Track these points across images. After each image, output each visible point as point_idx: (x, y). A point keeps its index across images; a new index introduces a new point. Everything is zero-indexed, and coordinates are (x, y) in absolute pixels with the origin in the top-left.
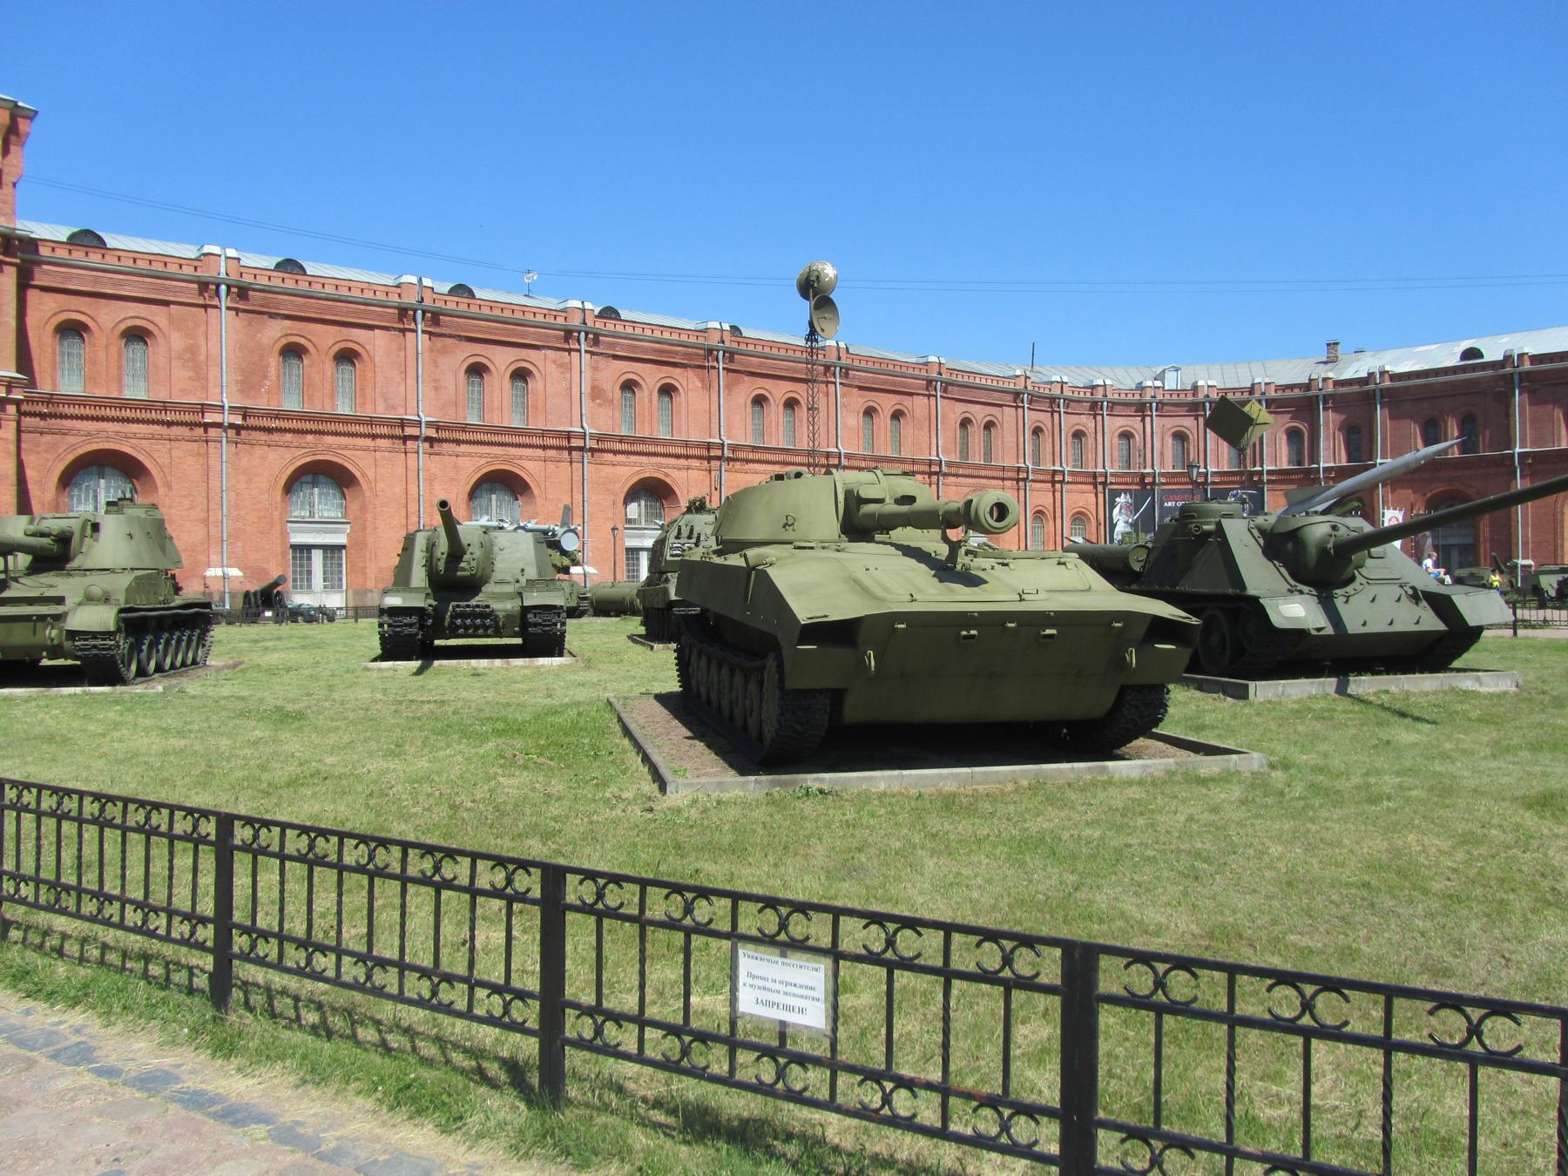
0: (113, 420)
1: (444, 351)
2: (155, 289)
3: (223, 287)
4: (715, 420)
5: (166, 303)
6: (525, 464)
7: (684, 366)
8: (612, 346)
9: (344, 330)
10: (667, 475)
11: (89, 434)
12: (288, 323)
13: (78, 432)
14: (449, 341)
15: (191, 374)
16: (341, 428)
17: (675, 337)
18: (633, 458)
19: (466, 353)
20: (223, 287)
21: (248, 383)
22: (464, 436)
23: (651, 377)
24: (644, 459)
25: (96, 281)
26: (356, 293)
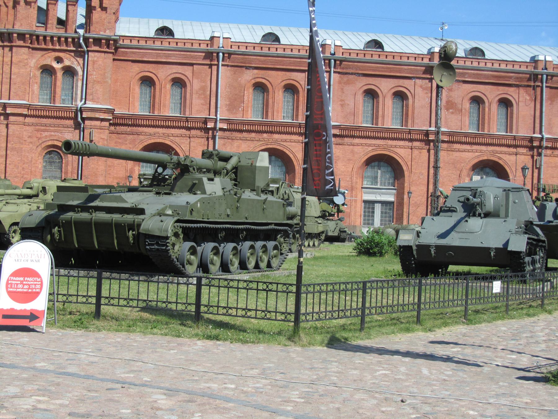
0: (162, 127)
1: (348, 83)
2: (186, 57)
3: (221, 54)
4: (537, 121)
5: (192, 65)
6: (398, 150)
8: (463, 75)
9: (288, 74)
10: (500, 158)
11: (150, 135)
12: (256, 71)
13: (146, 134)
14: (351, 76)
15: (202, 101)
16: (282, 129)
17: (510, 67)
18: (475, 147)
19: (362, 83)
20: (221, 54)
21: (232, 106)
22: (357, 133)
23: (491, 95)
24: (483, 148)
25: (158, 55)
26: (295, 52)
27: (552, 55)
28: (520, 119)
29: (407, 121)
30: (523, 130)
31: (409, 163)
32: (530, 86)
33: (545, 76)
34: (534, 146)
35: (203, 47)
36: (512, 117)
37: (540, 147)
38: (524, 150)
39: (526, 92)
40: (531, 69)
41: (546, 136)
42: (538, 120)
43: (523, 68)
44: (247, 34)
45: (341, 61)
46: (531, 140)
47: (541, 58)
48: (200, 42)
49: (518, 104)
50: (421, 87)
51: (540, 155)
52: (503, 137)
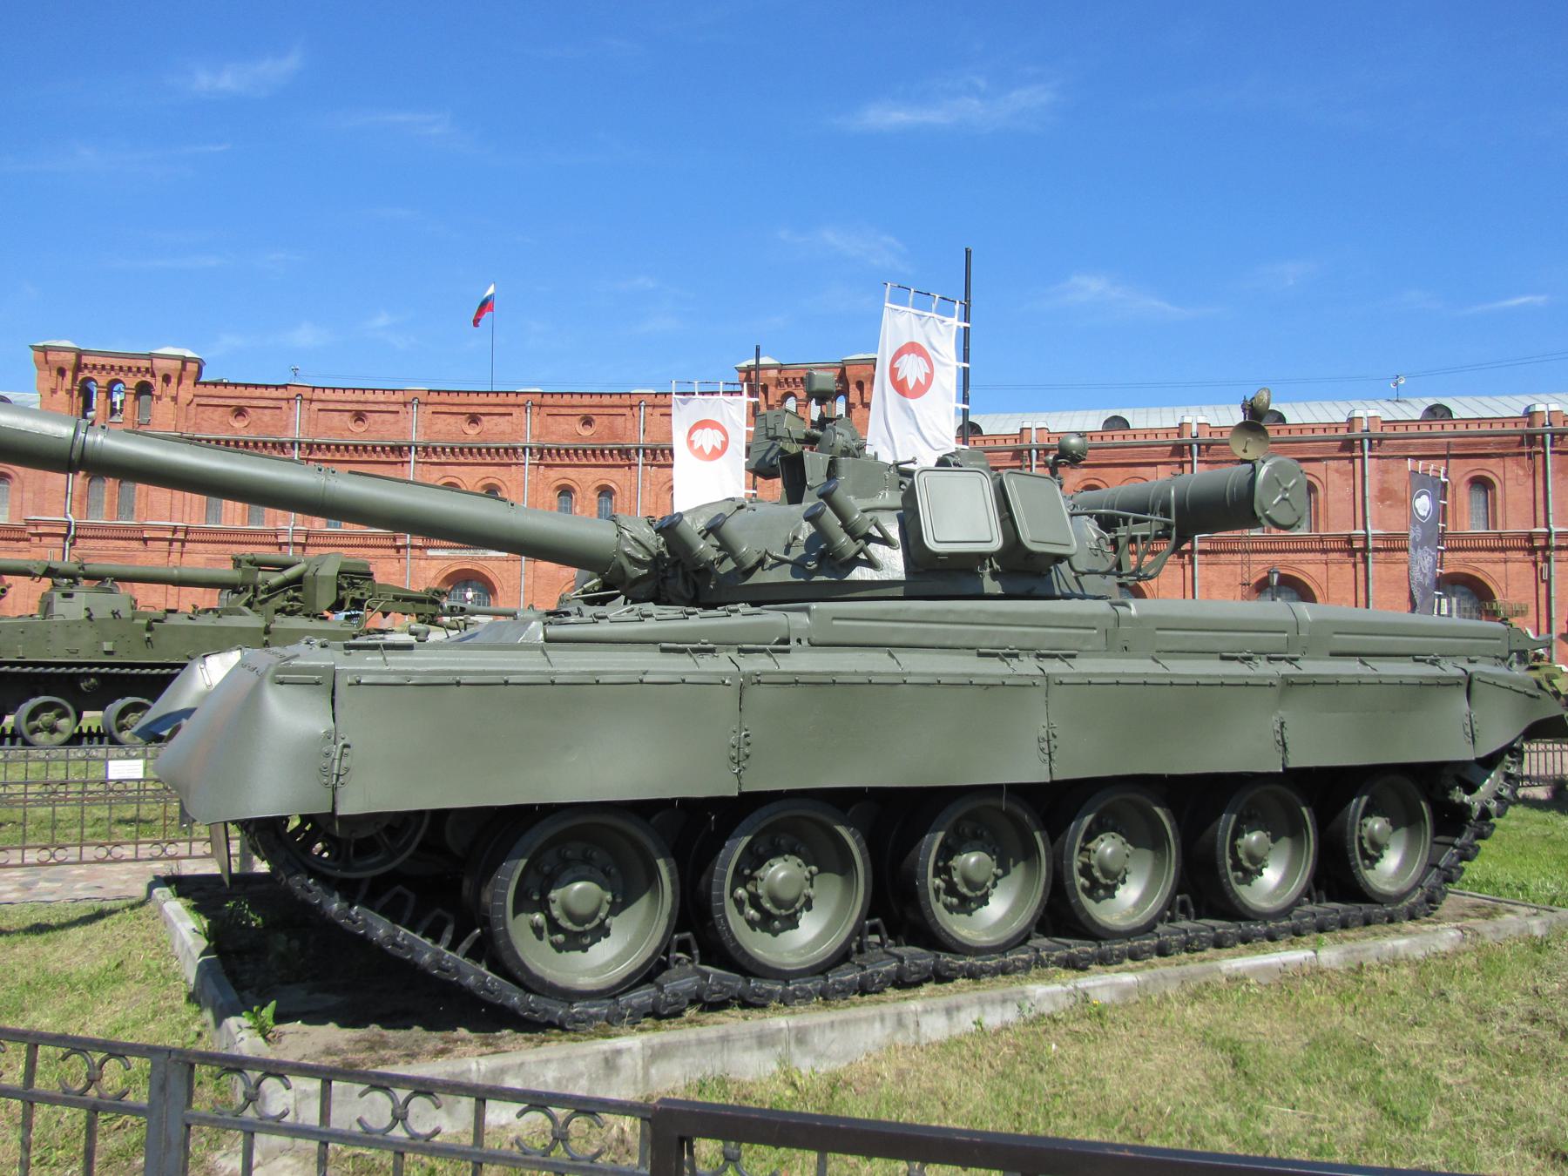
4: (1540, 507)
6: (1305, 568)
7: (1501, 456)
10: (1477, 569)
17: (1485, 428)
27: (1554, 404)
28: (1509, 507)
29: (1317, 524)
30: (1515, 522)
31: (1324, 586)
32: (1522, 454)
33: (1548, 437)
34: (1537, 548)
35: (1010, 443)
36: (1494, 505)
37: (1547, 547)
38: (1520, 555)
39: (1518, 464)
40: (1523, 427)
41: (1554, 529)
42: (1541, 505)
43: (1509, 428)
44: (1078, 422)
45: (1208, 446)
46: (1530, 537)
47: (1539, 408)
48: (1005, 437)
49: (1503, 484)
50: (1337, 471)
51: (1547, 560)
52: (1480, 536)
